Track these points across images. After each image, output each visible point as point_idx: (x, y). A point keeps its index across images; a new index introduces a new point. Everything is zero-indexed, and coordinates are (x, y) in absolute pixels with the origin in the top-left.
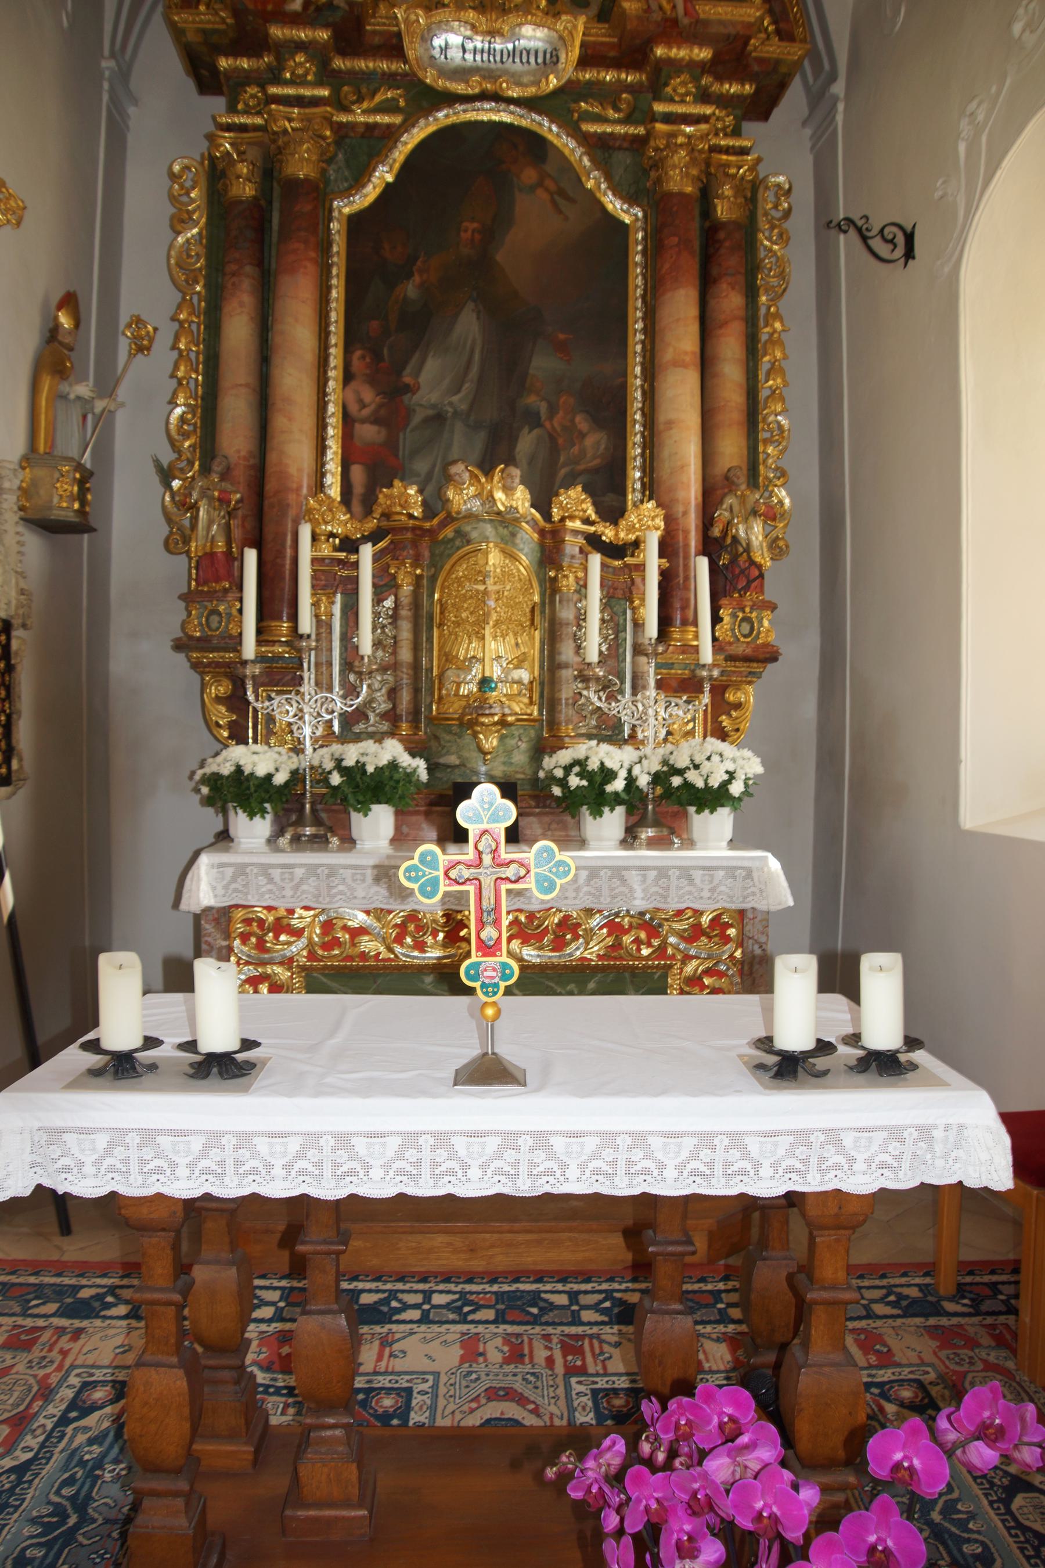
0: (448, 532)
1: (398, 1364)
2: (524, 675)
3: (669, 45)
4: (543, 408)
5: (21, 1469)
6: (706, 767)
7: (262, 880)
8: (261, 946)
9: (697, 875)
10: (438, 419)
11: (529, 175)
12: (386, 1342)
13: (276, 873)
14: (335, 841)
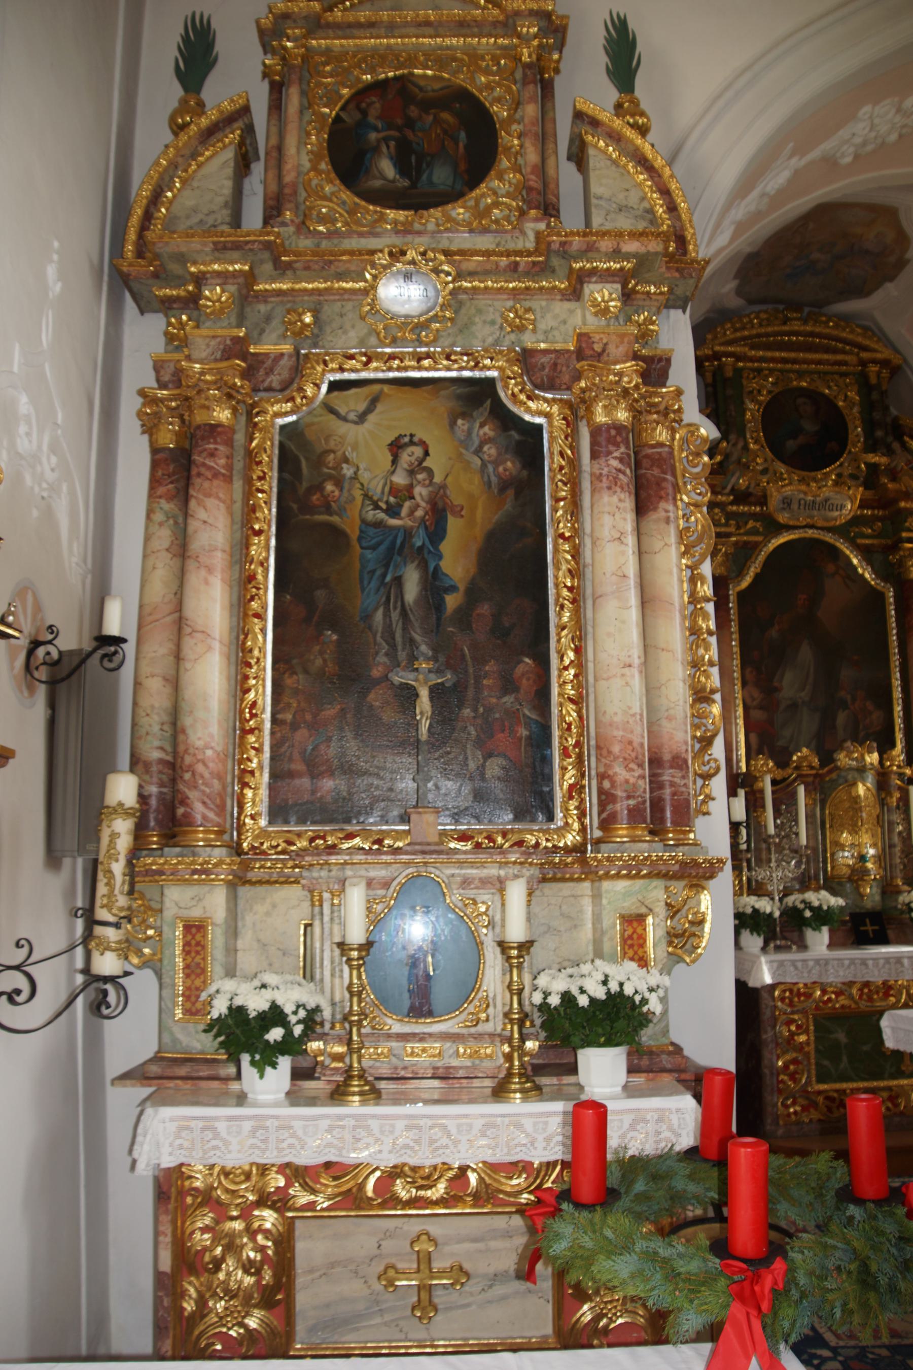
0: (834, 776)
3: (906, 501)
7: (792, 969)
10: (794, 707)
11: (831, 568)
13: (799, 964)
14: (794, 947)
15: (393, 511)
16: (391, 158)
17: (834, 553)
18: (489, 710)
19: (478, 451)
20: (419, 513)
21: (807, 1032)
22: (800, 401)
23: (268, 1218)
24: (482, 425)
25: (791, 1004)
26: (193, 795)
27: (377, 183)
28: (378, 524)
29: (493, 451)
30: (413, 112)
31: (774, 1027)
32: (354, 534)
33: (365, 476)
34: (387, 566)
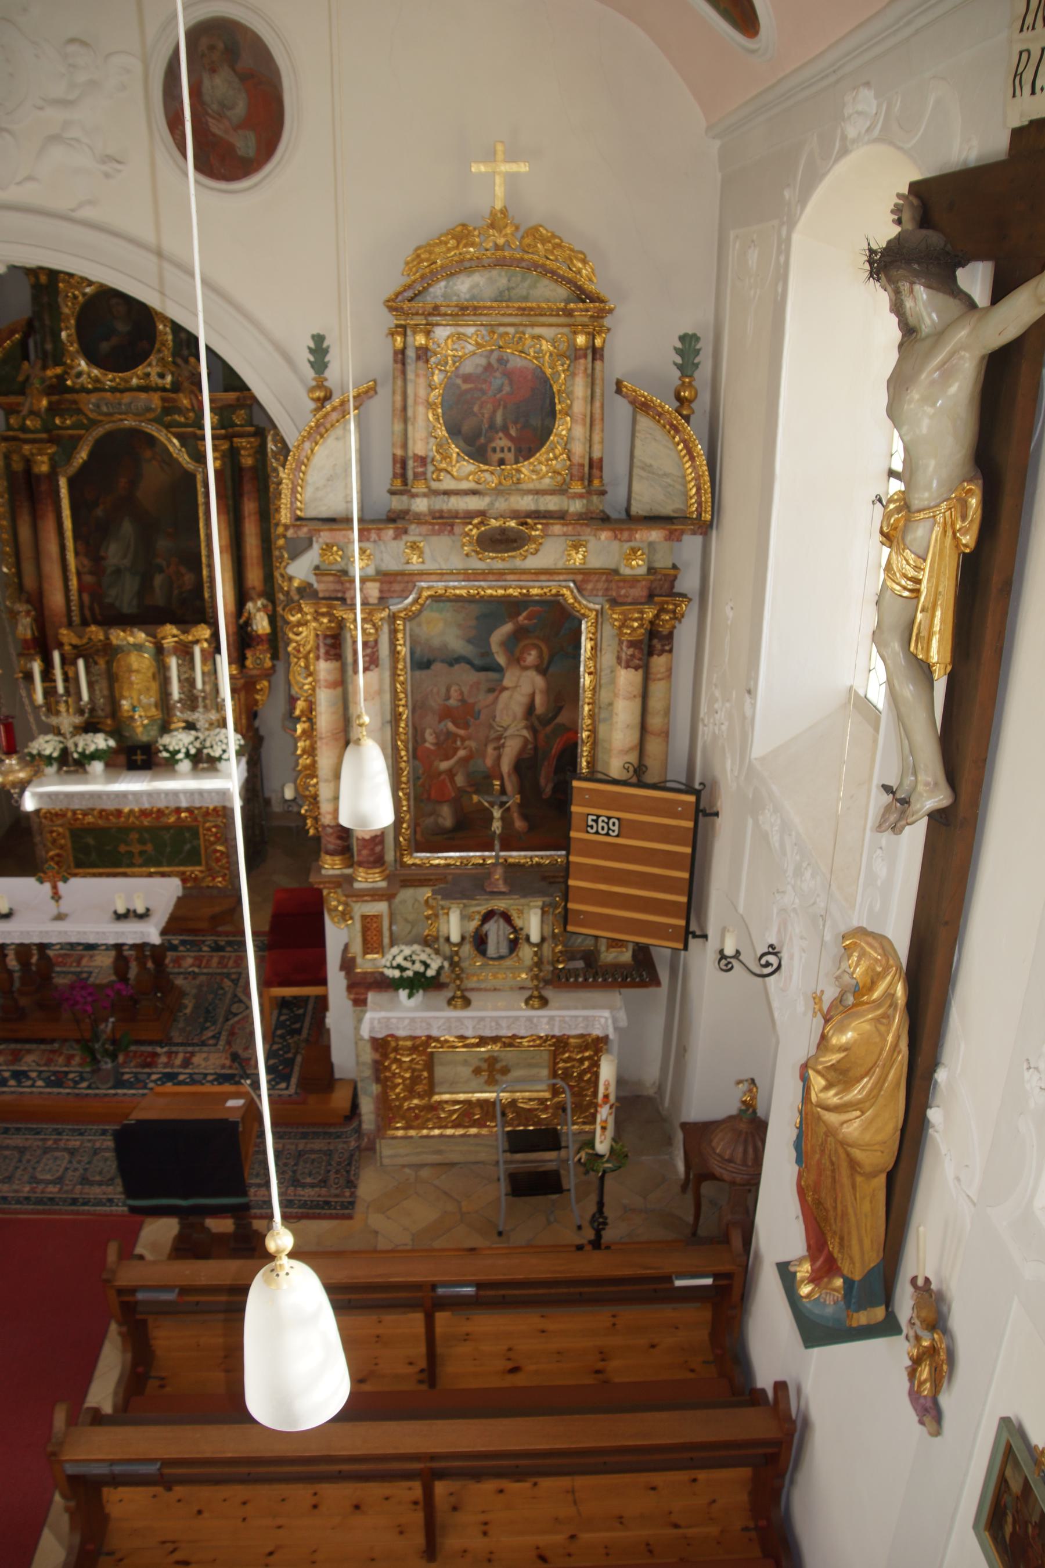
2: (153, 700)
4: (164, 563)
6: (215, 747)
9: (206, 795)
10: (118, 572)
11: (148, 454)
12: (91, 957)
17: (151, 440)
21: (64, 837)
22: (114, 301)
31: (41, 834)
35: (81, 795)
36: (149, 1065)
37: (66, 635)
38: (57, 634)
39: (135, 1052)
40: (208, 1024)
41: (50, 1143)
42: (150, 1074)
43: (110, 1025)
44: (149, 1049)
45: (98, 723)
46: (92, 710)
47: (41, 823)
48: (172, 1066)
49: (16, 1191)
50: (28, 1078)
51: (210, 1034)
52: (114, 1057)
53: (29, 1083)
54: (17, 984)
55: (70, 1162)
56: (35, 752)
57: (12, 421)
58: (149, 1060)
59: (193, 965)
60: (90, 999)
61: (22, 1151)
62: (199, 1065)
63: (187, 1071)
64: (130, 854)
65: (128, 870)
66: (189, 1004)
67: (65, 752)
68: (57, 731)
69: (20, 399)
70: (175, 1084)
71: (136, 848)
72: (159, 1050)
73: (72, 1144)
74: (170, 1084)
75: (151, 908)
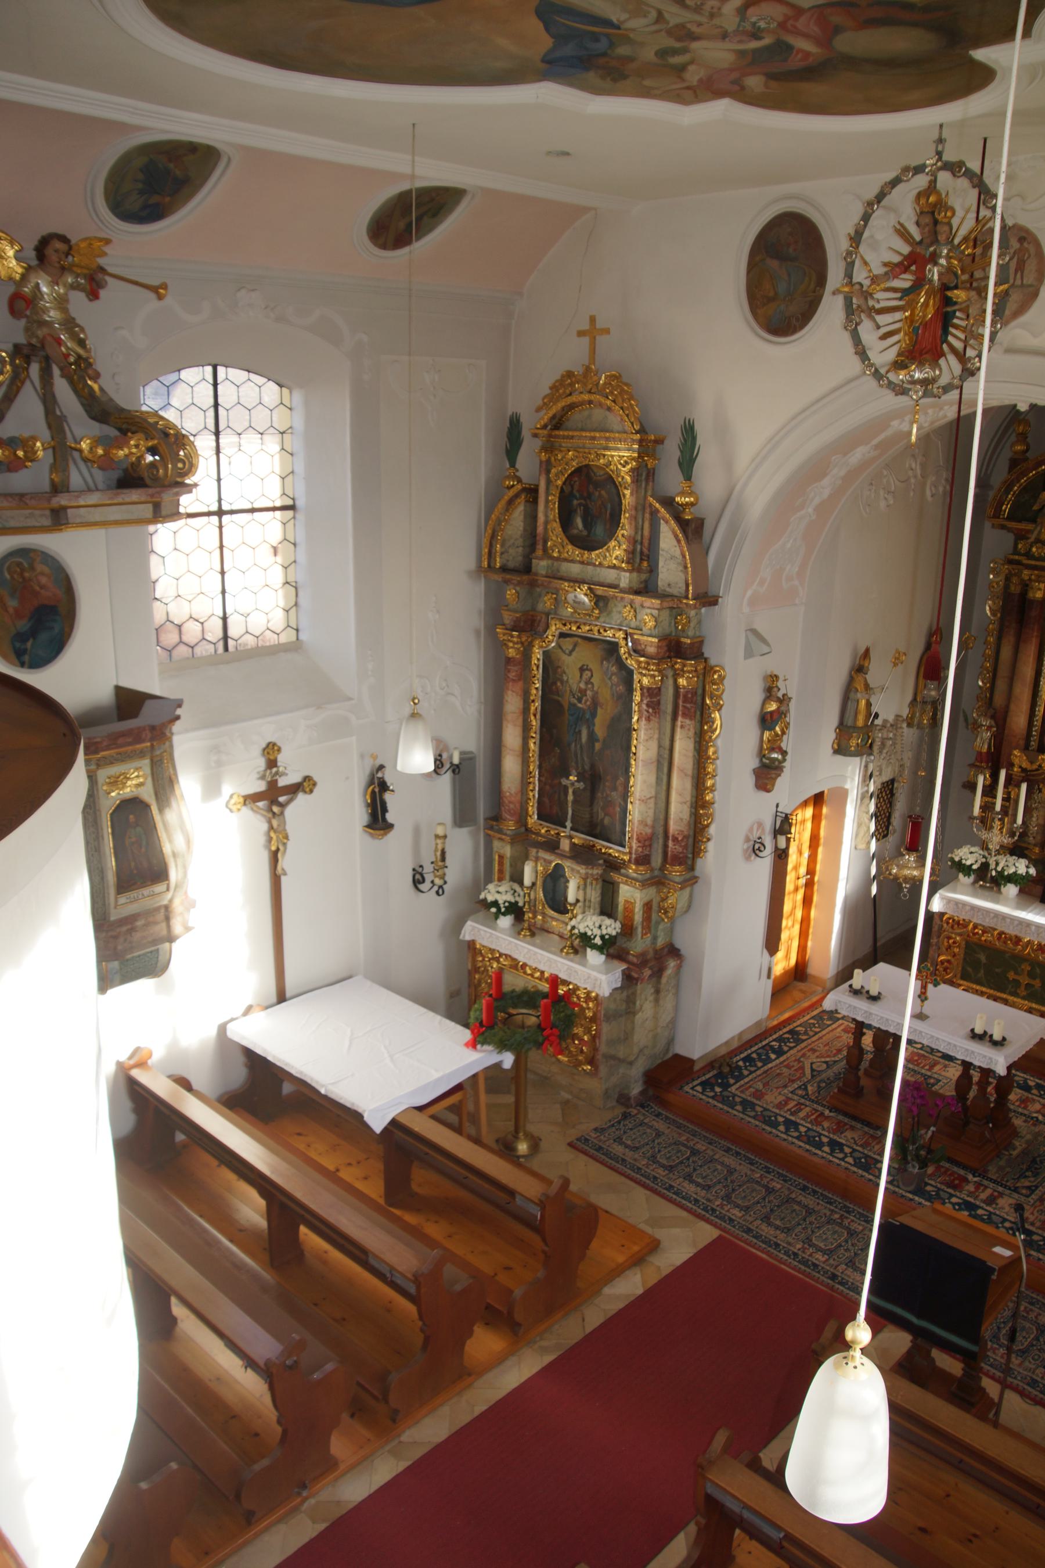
1: (943, 1073)
5: (835, 1062)
8: (952, 927)
12: (946, 1066)
15: (580, 700)
16: (581, 517)
18: (607, 796)
19: (610, 679)
20: (588, 703)
21: (959, 947)
23: (495, 965)
24: (612, 666)
25: (952, 927)
26: (503, 808)
27: (575, 531)
28: (574, 705)
29: (616, 680)
30: (591, 488)
31: (939, 937)
32: (566, 707)
33: (571, 681)
34: (576, 725)
35: (988, 911)
36: (955, 1187)
37: (1018, 758)
38: (1010, 754)
39: (947, 1170)
40: (1029, 1174)
41: (837, 1216)
42: (951, 1196)
43: (930, 1133)
44: (962, 1172)
45: (1027, 849)
46: (1023, 835)
47: (942, 926)
48: (976, 1198)
49: (789, 1244)
50: (842, 1151)
51: (1027, 1184)
52: (923, 1165)
53: (841, 1156)
54: (865, 1065)
55: (846, 1241)
56: (957, 859)
57: (1020, 546)
58: (957, 1182)
59: (1038, 1112)
60: (918, 1101)
61: (810, 1212)
62: (1003, 1208)
63: (988, 1208)
64: (1017, 983)
65: (1011, 998)
66: (1019, 1145)
67: (985, 866)
68: (984, 846)
69: (1030, 526)
70: (970, 1215)
71: (1025, 980)
72: (970, 1177)
73: (854, 1226)
74: (966, 1213)
75: (1006, 1036)
